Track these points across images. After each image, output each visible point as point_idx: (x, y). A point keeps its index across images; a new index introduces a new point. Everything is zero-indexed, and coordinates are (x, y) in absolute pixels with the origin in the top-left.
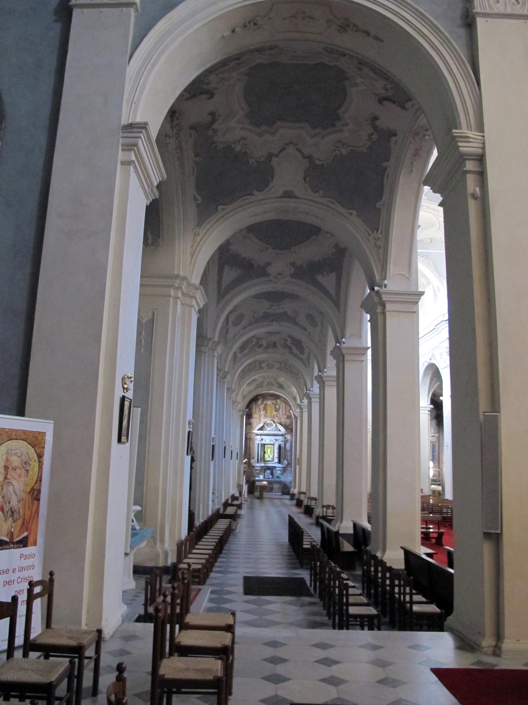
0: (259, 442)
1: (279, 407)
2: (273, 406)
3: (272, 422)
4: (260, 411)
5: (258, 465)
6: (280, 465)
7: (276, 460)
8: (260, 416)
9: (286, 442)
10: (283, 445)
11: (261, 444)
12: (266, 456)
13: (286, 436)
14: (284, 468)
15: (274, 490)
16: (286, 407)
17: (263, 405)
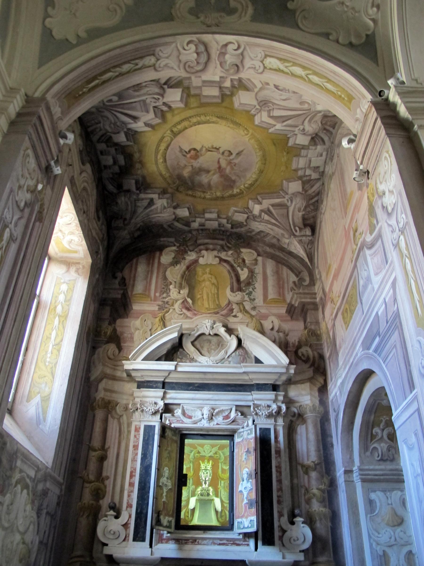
0: (155, 422)
1: (252, 272)
2: (224, 270)
3: (222, 331)
4: (166, 290)
6: (268, 553)
7: (248, 520)
8: (165, 307)
9: (294, 419)
10: (278, 429)
11: (164, 428)
16: (277, 273)
17: (181, 268)
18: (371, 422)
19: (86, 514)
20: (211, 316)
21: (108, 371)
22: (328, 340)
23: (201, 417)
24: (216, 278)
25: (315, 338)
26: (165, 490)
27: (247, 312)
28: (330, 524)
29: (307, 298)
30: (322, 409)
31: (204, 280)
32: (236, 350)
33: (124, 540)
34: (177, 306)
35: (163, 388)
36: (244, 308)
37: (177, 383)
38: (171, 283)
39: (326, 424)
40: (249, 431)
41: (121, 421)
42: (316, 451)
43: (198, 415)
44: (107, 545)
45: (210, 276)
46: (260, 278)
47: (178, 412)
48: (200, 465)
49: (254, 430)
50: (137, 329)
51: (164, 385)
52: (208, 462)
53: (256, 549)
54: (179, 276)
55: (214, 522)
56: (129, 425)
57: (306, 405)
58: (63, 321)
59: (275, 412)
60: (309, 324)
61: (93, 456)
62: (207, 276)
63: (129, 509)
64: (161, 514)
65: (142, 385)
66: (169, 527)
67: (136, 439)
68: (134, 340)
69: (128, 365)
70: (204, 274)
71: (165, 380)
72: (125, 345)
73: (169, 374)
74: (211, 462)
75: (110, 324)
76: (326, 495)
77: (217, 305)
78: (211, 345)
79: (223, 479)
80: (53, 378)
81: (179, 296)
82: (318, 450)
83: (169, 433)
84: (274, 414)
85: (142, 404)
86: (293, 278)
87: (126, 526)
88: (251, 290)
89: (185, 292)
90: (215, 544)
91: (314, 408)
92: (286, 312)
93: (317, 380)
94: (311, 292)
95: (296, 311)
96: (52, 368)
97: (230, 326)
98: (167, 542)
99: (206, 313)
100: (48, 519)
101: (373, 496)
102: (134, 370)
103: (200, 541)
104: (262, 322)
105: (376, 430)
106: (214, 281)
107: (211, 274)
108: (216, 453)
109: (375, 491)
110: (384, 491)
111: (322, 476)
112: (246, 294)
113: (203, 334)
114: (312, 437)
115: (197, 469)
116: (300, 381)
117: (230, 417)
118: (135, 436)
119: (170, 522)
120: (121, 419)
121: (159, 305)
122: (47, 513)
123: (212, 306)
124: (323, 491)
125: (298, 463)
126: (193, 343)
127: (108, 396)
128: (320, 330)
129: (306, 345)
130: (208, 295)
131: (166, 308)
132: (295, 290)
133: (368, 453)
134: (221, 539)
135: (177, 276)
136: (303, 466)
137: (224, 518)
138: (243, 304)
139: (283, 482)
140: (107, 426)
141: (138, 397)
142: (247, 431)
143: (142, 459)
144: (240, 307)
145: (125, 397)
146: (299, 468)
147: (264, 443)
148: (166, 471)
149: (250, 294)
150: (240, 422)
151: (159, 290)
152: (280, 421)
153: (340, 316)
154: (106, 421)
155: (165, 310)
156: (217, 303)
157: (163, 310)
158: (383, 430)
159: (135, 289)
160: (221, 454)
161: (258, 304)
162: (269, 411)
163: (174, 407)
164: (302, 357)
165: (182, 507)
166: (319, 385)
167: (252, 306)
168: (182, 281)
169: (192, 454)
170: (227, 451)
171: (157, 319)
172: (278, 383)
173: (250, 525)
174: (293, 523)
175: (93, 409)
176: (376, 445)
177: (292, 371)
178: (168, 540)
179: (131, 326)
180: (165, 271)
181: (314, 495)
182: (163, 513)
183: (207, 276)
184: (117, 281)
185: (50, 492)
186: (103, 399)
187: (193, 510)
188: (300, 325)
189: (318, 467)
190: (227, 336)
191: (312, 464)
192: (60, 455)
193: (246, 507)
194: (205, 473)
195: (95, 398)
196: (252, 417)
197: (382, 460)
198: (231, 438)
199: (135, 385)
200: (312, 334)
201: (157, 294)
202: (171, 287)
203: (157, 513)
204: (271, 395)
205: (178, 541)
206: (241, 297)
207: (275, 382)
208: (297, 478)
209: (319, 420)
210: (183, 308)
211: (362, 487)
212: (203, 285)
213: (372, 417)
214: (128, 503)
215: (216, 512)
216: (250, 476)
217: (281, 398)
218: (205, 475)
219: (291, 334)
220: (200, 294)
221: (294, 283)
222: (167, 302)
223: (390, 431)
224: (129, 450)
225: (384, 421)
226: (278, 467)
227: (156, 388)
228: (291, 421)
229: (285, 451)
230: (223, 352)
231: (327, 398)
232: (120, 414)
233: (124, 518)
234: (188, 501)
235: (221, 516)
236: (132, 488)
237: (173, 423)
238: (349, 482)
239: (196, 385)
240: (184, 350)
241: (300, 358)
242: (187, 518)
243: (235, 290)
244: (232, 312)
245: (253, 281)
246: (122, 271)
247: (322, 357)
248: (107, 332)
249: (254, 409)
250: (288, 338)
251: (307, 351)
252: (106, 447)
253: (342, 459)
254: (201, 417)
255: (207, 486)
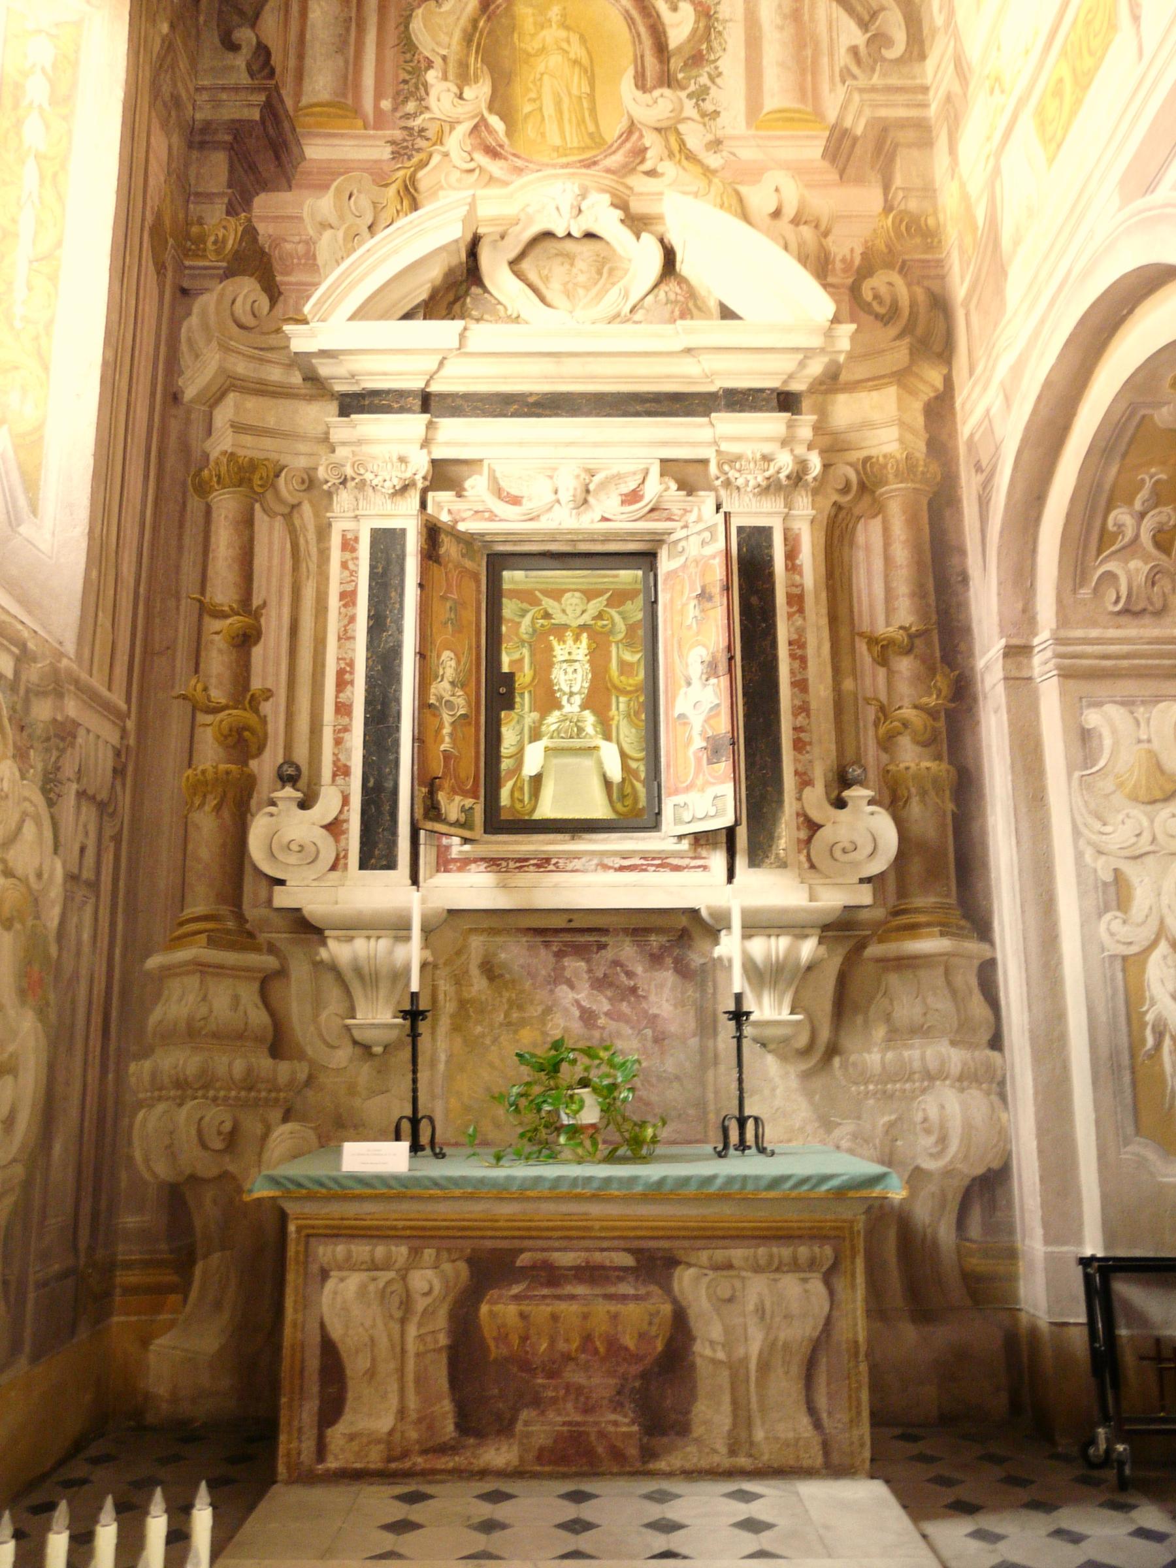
0: (405, 518)
5: (384, 891)
6: (767, 888)
7: (706, 795)
8: (410, 147)
11: (433, 533)
12: (529, 753)
13: (846, 410)
14: (840, 929)
15: (712, 1416)
18: (1107, 487)
19: (212, 802)
20: (573, 174)
21: (241, 367)
22: (968, 240)
23: (553, 497)
24: (583, 39)
25: (918, 240)
26: (447, 719)
27: (691, 157)
28: (950, 806)
29: (895, 105)
30: (934, 467)
31: (543, 50)
32: (656, 286)
33: (333, 868)
34: (456, 141)
35: (425, 408)
36: (682, 143)
37: (466, 397)
38: (430, 65)
39: (947, 513)
40: (707, 535)
41: (297, 522)
42: (913, 595)
43: (537, 494)
44: (282, 882)
45: (563, 34)
46: (734, 37)
47: (476, 485)
48: (551, 649)
49: (722, 528)
50: (325, 226)
51: (427, 402)
52: (577, 639)
53: (731, 876)
54: (457, 35)
55: (599, 809)
56: (323, 532)
57: (885, 456)
58: (55, 175)
59: (788, 477)
60: (901, 194)
61: (217, 633)
62: (552, 34)
63: (340, 780)
64: (440, 788)
65: (356, 403)
66: (465, 824)
67: (347, 573)
68: (320, 262)
69: (301, 340)
70: (542, 27)
71: (427, 384)
72: (292, 279)
73: (441, 364)
74: (585, 636)
75: (231, 211)
76: (941, 724)
77: (591, 135)
78: (575, 270)
79: (622, 691)
80: (46, 369)
81: (460, 110)
82: (919, 593)
83: (448, 548)
84: (784, 482)
85: (358, 464)
86: (851, 34)
87: (334, 827)
88: (704, 80)
89: (479, 92)
90: (606, 867)
91: (909, 468)
92: (823, 156)
93: (922, 379)
94: (909, 82)
95: (858, 150)
96: (37, 338)
97: (636, 207)
98: (460, 869)
99: (554, 166)
100: (89, 813)
101: (1093, 718)
102: (323, 353)
103: (561, 863)
104: (744, 190)
105: (1121, 516)
106: (576, 50)
107: (568, 28)
108: (600, 616)
109: (1099, 704)
110: (1127, 703)
111: (932, 671)
112: (689, 96)
113: (548, 235)
114: (901, 554)
115: (544, 663)
116: (869, 380)
117: (641, 498)
118: (344, 565)
119: (468, 811)
120: (295, 515)
121: (393, 143)
122: (81, 794)
123: (573, 141)
124: (932, 713)
125: (855, 633)
126: (513, 263)
127: (251, 447)
128: (935, 213)
129: (889, 266)
130: (558, 104)
131: (419, 150)
132: (855, 77)
133: (1085, 592)
134: (625, 855)
135: (451, 36)
136: (872, 641)
137: (629, 802)
138: (678, 133)
139: (811, 689)
140: (251, 540)
141: (344, 444)
142: (698, 533)
143: (370, 630)
144: (667, 140)
145: (302, 447)
146: (862, 646)
147: (752, 568)
148: (448, 664)
149: (700, 95)
150: (676, 509)
151: (390, 90)
152: (804, 508)
153: (1027, 122)
154: (247, 523)
155: (415, 160)
156: (592, 129)
157: (410, 158)
158: (1142, 515)
159: (307, 86)
160: (617, 618)
161: (729, 131)
162: (767, 474)
163: (464, 469)
164: (875, 305)
165: (503, 774)
166: (927, 394)
167: (710, 137)
168: (468, 55)
169: (526, 621)
170: (635, 610)
171: (392, 191)
172: (796, 386)
173: (712, 812)
174: (840, 804)
175: (202, 489)
176: (1111, 566)
177: (844, 344)
178: (464, 863)
179: (305, 215)
180: (406, 20)
181: (905, 724)
182: (446, 784)
183: (552, 34)
184: (240, 61)
185: (81, 732)
186: (232, 456)
187: (537, 780)
188: (869, 199)
189: (917, 642)
190: (626, 234)
191: (900, 636)
192: (104, 620)
193: (698, 760)
194: (570, 670)
195: (206, 456)
196: (712, 494)
197: (1126, 611)
198: (648, 559)
199: (333, 407)
200: (908, 228)
201: (386, 104)
202: (431, 76)
203: (429, 786)
204: (773, 423)
205: (494, 863)
206: (670, 107)
207: (785, 382)
208: (855, 679)
209: (925, 502)
210: (474, 148)
211: (1063, 693)
212: (541, 68)
213: (1114, 470)
214: (335, 763)
215: (608, 784)
216: (711, 669)
217: (805, 432)
218: (571, 671)
219: (836, 231)
220: (534, 100)
221: (854, 51)
222: (422, 130)
223: (1164, 518)
224: (326, 609)
225: (1148, 484)
226: (797, 644)
227: (402, 410)
228: (838, 507)
229: (817, 597)
230: (614, 293)
231: (953, 434)
232: (295, 502)
233: (327, 805)
234: (519, 756)
235: (623, 797)
236: (346, 720)
237: (463, 520)
238: (1019, 683)
239: (531, 400)
240: (486, 290)
241: (866, 308)
242: (518, 806)
243: (649, 84)
244: (643, 161)
245: (710, 49)
246: (253, 21)
247: (940, 305)
248: (224, 241)
249: (720, 466)
250: (829, 242)
251: (890, 284)
252: (256, 602)
253: (1000, 613)
254: (553, 497)
255: (575, 708)
